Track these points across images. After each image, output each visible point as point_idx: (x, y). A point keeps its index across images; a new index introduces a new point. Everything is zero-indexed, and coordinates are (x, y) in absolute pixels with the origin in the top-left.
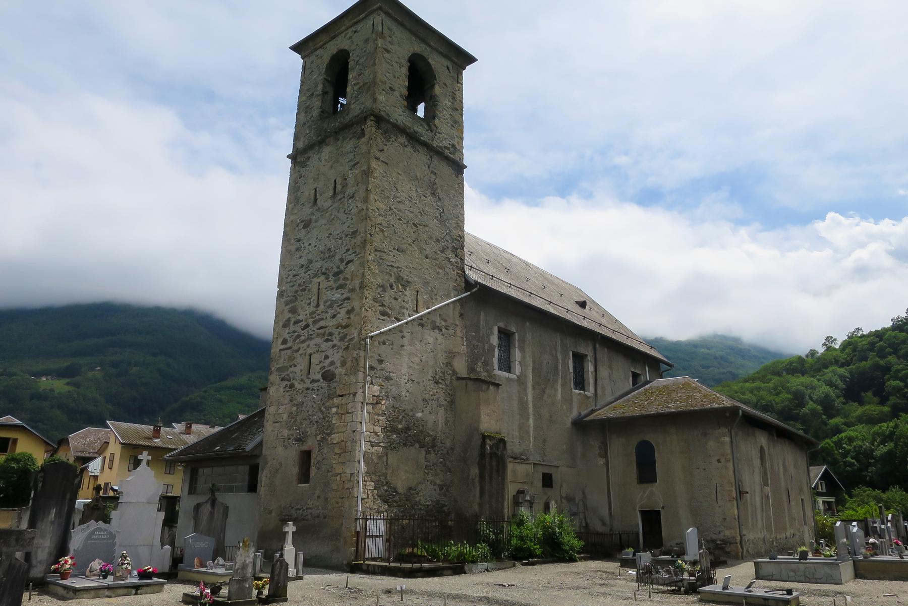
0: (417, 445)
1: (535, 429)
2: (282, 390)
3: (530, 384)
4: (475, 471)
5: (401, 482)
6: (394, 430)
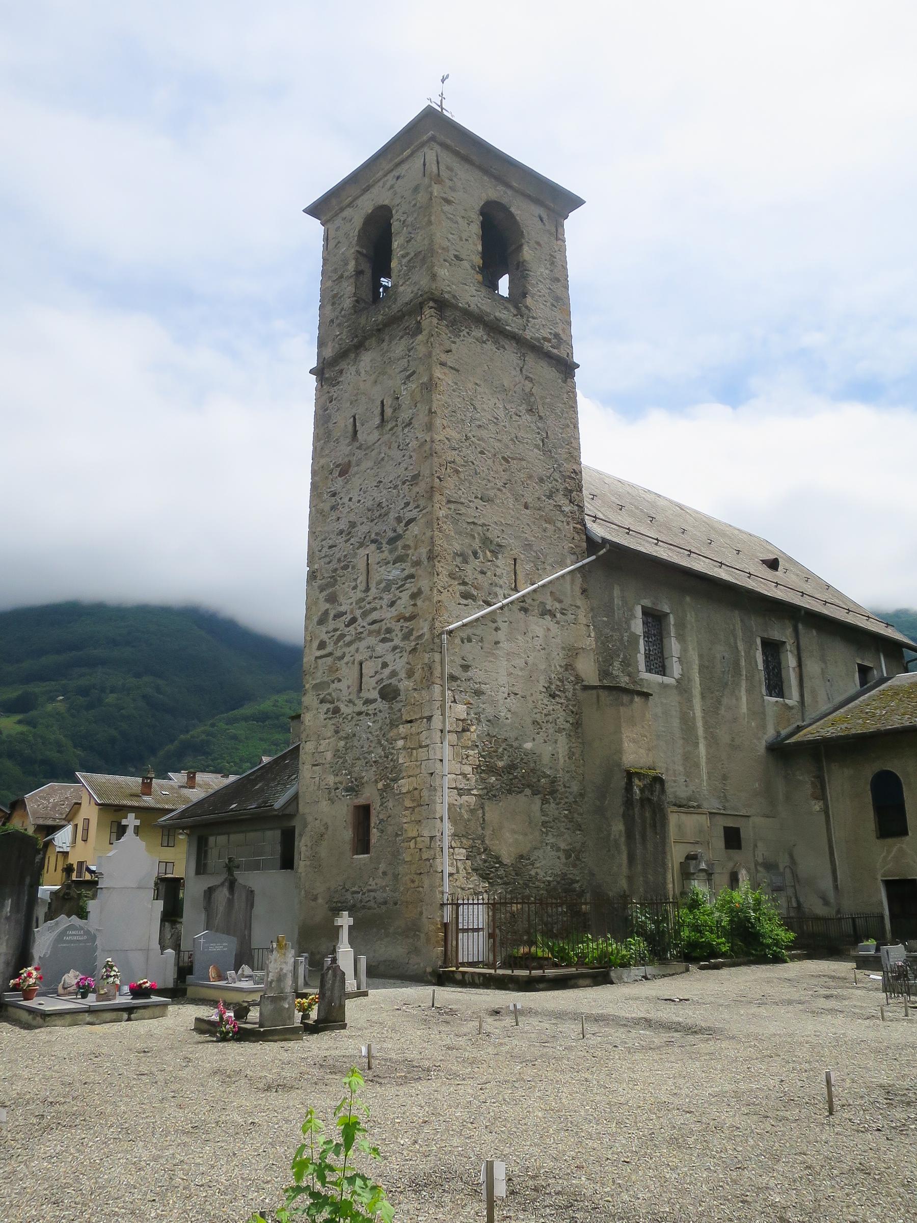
1: (709, 760)
2: (322, 716)
3: (696, 691)
4: (618, 827)
5: (507, 848)
6: (492, 770)
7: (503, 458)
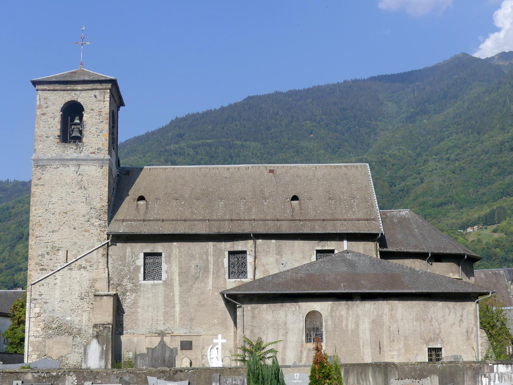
0: (67, 334)
1: (181, 313)
7: (64, 213)
